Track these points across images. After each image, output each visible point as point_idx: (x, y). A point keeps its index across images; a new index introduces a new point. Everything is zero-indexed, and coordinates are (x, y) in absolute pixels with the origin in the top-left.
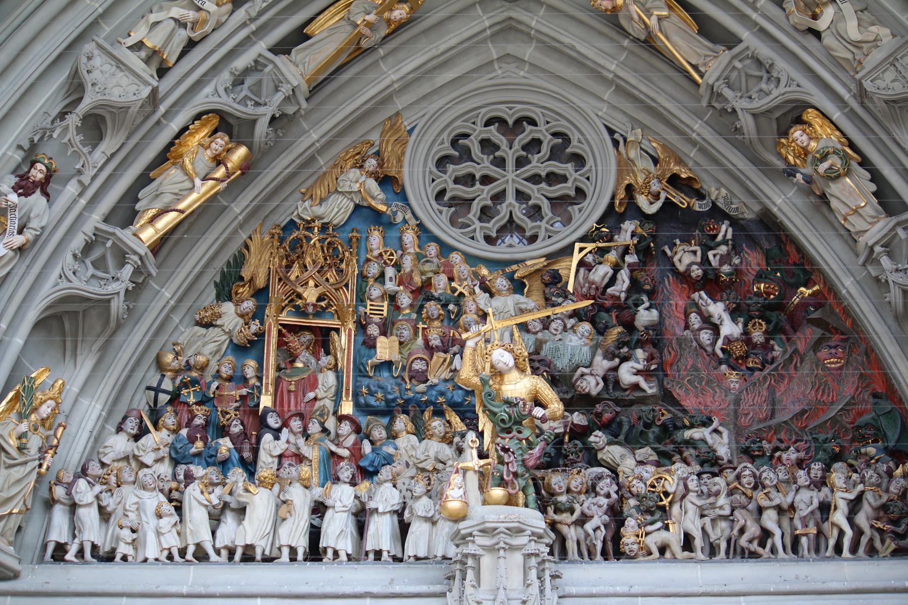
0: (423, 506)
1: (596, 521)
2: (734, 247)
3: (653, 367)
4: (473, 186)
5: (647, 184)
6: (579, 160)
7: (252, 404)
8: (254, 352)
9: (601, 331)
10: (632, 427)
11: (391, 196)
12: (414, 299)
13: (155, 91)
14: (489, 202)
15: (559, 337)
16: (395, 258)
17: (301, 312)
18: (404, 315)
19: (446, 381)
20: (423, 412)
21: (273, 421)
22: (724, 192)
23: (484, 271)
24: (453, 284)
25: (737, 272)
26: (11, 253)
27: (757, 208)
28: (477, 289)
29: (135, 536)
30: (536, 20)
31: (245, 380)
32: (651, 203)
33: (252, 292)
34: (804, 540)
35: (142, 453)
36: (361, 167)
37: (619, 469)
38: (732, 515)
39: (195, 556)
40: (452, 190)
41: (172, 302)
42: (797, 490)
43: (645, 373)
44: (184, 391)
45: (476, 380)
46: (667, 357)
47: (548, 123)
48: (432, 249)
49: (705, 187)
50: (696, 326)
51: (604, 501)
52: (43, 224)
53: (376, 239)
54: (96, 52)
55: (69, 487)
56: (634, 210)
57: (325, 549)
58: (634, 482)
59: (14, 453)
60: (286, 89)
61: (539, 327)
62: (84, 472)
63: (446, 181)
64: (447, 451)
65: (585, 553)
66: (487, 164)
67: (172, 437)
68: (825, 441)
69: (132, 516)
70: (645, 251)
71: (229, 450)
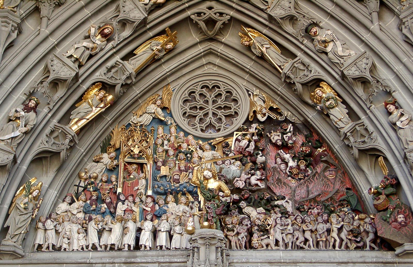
0: (178, 229)
1: (242, 235)
2: (293, 134)
3: (263, 178)
5: (261, 110)
6: (235, 101)
8: (115, 172)
10: (255, 200)
11: (166, 114)
12: (175, 153)
13: (77, 74)
14: (202, 117)
15: (229, 166)
16: (168, 137)
17: (133, 157)
18: (171, 158)
19: (186, 182)
20: (178, 194)
21: (122, 197)
22: (290, 113)
23: (201, 142)
24: (189, 147)
25: (295, 142)
26: (22, 134)
27: (302, 119)
28: (198, 149)
29: (69, 241)
30: (220, 49)
31: (112, 182)
32: (263, 117)
33: (114, 150)
34: (321, 243)
35: (72, 210)
36: (155, 104)
38: (293, 233)
39: (92, 248)
40: (189, 112)
41: (84, 153)
42: (318, 224)
44: (89, 187)
45: (198, 182)
46: (268, 174)
47: (224, 88)
48: (182, 134)
49: (282, 111)
50: (279, 163)
52: (35, 123)
53: (161, 130)
57: (141, 245)
58: (257, 220)
60: (127, 74)
61: (221, 162)
62: (50, 217)
63: (186, 109)
64: (187, 209)
65: (239, 248)
66: (202, 103)
67: (84, 203)
68: (328, 206)
70: (260, 135)
71: (105, 208)
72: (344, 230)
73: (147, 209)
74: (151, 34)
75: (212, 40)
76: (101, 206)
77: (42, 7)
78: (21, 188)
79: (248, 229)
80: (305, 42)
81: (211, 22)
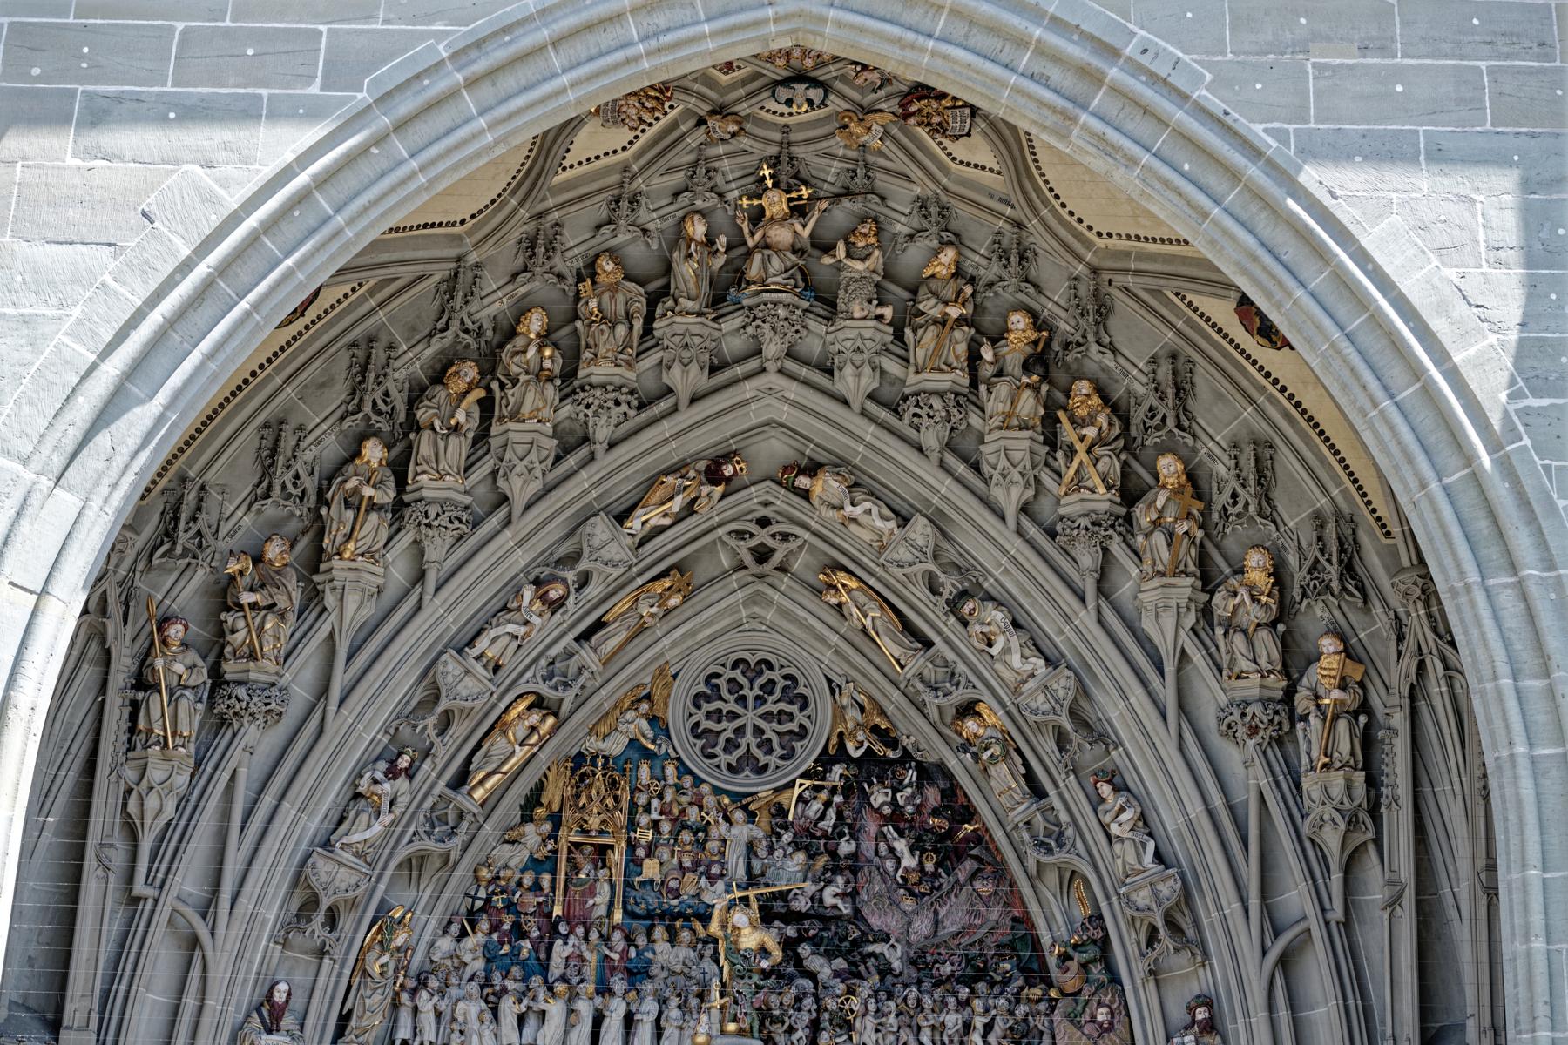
1: (800, 1033)
4: (719, 721)
9: (812, 856)
23: (727, 801)
25: (919, 808)
43: (843, 895)
48: (687, 781)
51: (806, 1018)
53: (645, 772)
56: (842, 755)
70: (847, 791)
72: (996, 1027)
79: (812, 1021)
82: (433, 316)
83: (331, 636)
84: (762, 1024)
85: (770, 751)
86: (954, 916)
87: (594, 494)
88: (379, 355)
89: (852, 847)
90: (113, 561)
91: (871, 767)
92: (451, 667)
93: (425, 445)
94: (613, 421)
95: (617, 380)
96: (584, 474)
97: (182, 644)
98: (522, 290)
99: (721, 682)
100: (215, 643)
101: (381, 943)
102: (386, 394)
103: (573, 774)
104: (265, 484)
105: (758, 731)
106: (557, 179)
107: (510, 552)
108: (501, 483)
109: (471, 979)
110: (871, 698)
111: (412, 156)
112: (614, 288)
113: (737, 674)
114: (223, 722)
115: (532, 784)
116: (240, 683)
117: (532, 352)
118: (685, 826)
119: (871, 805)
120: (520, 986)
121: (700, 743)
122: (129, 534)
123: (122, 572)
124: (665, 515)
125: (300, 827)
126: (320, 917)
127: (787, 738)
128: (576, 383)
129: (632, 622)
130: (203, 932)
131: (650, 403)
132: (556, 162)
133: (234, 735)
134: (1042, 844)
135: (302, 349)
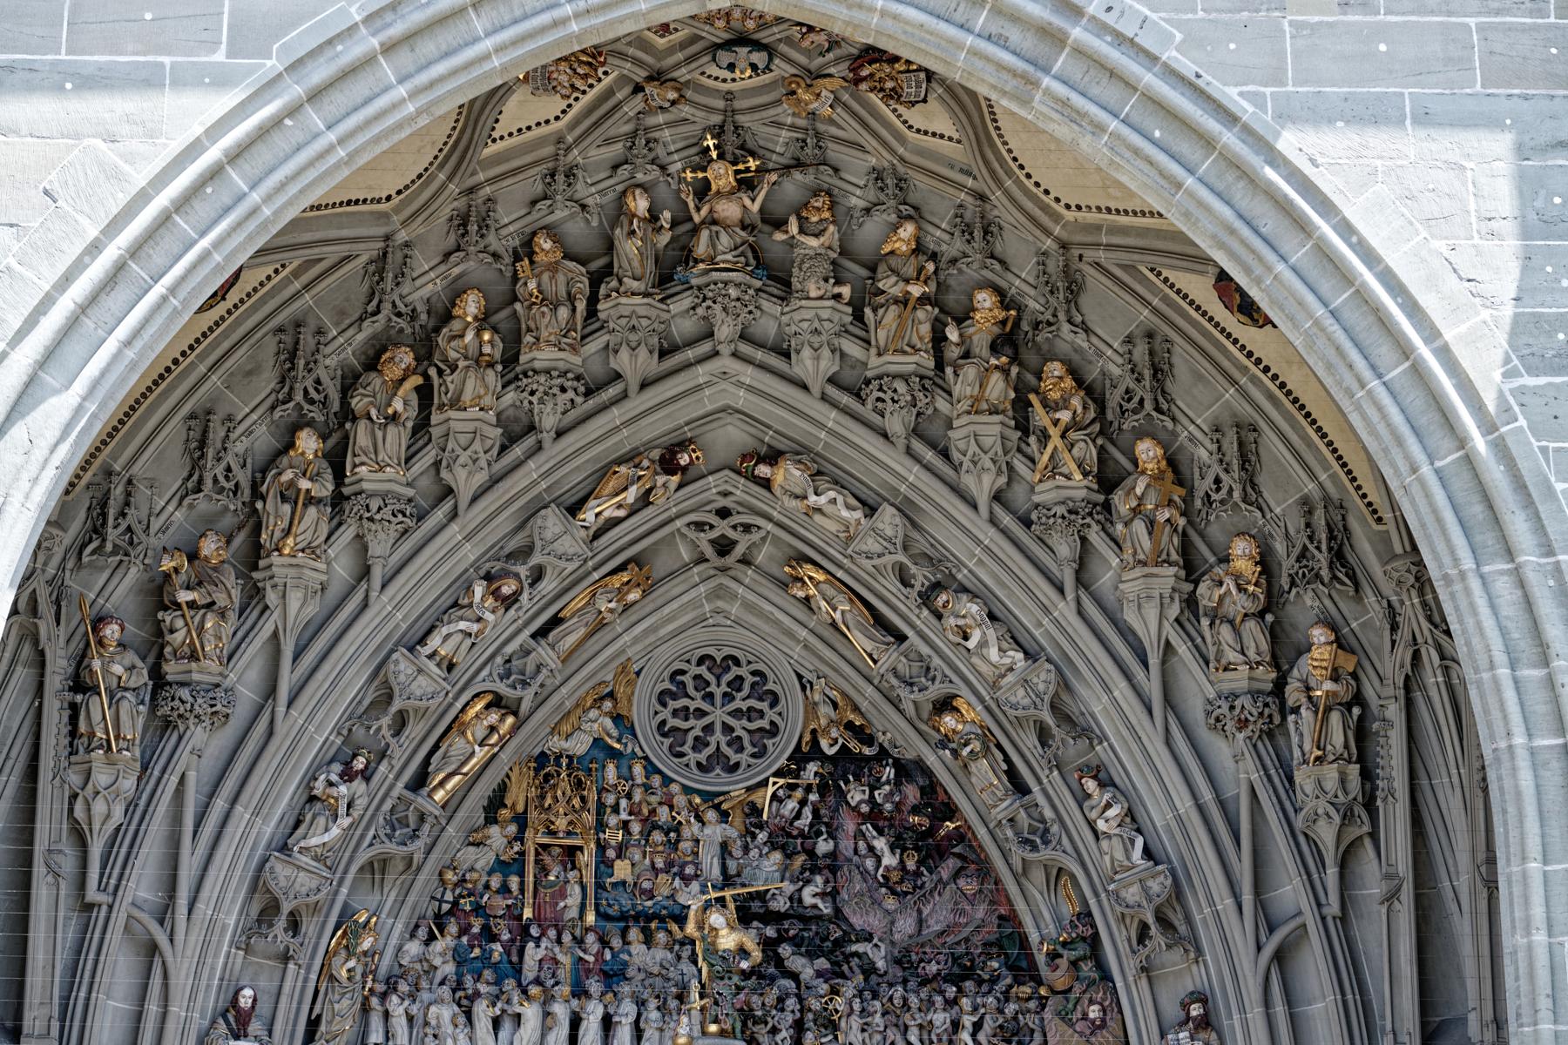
1: (784, 1034)
4: (687, 719)
7: (516, 913)
8: (515, 867)
9: (789, 856)
21: (534, 931)
23: (698, 800)
25: (898, 806)
31: (509, 891)
37: (802, 977)
43: (822, 895)
48: (656, 781)
51: (790, 1018)
53: (611, 772)
54: (401, 659)
55: (384, 996)
56: (816, 752)
59: (345, 983)
64: (669, 956)
69: (433, 1022)
70: (823, 789)
72: (986, 1026)
73: (587, 957)
74: (596, 576)
75: (724, 570)
76: (492, 951)
77: (369, 538)
78: (339, 933)
80: (925, 612)
81: (723, 547)
82: (363, 299)
83: (275, 634)
84: (744, 1024)
85: (741, 749)
86: (938, 915)
87: (544, 485)
88: (308, 340)
89: (830, 845)
90: (41, 559)
91: (846, 764)
92: (402, 666)
93: (362, 436)
94: (560, 409)
95: (561, 365)
96: (531, 464)
97: (119, 645)
98: (456, 271)
99: (687, 679)
100: (154, 643)
101: (347, 947)
102: (318, 382)
103: (536, 775)
104: (195, 477)
105: (728, 729)
106: (487, 152)
107: (458, 546)
108: (444, 474)
109: (442, 983)
110: (844, 694)
111: (329, 128)
112: (553, 268)
113: (703, 670)
114: (167, 725)
115: (495, 786)
116: (182, 684)
117: (470, 336)
118: (655, 826)
119: (848, 803)
120: (493, 989)
121: (667, 742)
122: (55, 531)
123: (51, 571)
124: (620, 506)
125: (255, 831)
126: (281, 923)
127: (757, 736)
128: (518, 369)
129: (590, 617)
130: (162, 938)
131: (598, 389)
132: (485, 133)
133: (180, 738)
134: (1026, 841)
135: (225, 335)
